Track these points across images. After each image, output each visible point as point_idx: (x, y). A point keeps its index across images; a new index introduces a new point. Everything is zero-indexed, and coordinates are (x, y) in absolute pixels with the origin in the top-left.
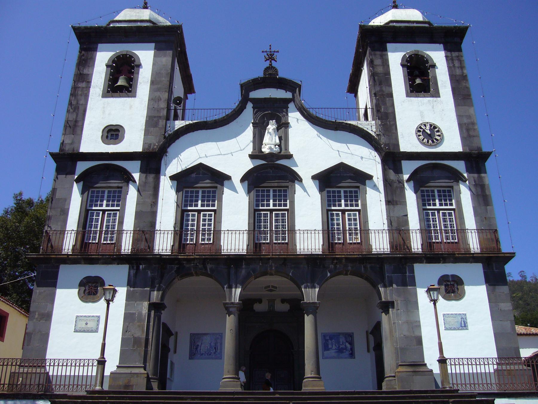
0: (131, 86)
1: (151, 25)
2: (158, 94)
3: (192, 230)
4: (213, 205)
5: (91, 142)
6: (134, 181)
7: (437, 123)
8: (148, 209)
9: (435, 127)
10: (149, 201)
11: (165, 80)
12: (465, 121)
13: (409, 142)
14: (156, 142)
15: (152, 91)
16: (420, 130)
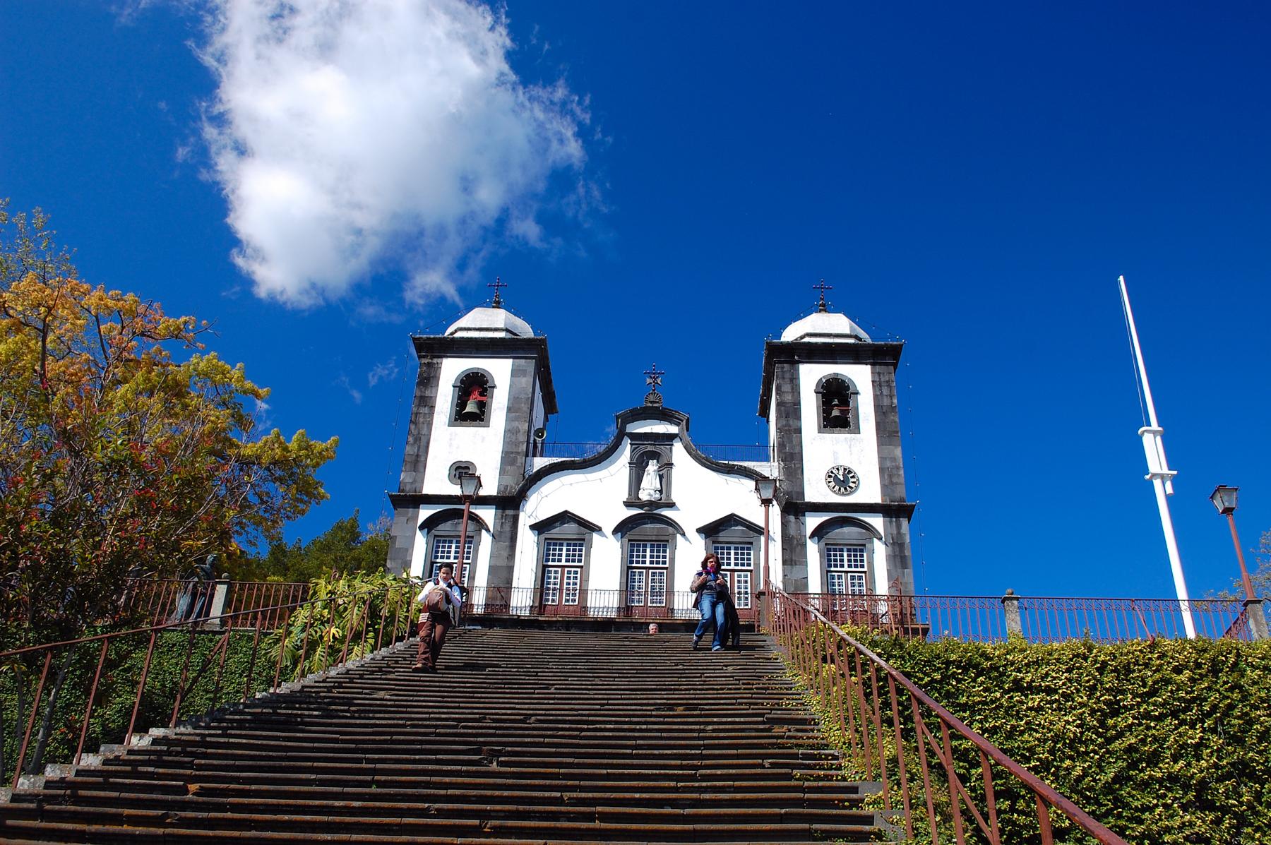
0: (483, 413)
1: (510, 336)
2: (516, 424)
3: (554, 589)
4: (580, 561)
5: (436, 481)
6: (488, 530)
7: (854, 467)
8: (503, 563)
9: (850, 472)
10: (505, 554)
11: (525, 408)
12: (888, 464)
13: (816, 490)
14: (514, 486)
15: (509, 420)
16: (831, 475)
